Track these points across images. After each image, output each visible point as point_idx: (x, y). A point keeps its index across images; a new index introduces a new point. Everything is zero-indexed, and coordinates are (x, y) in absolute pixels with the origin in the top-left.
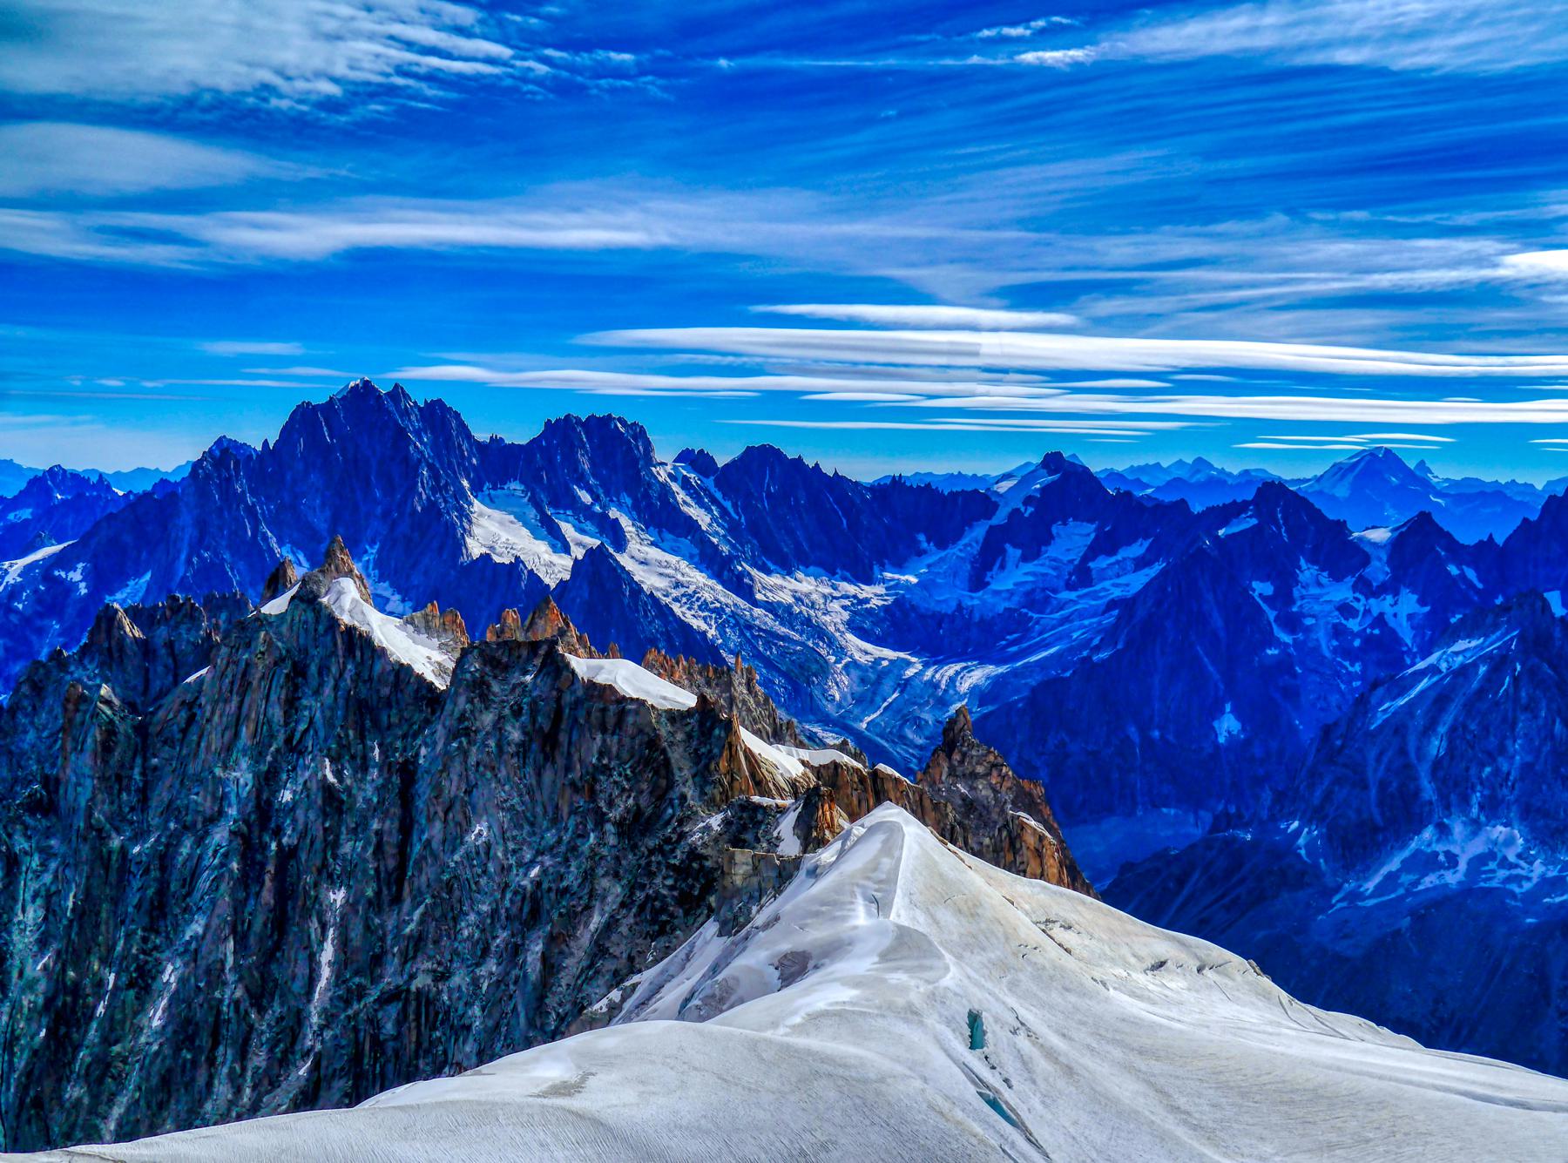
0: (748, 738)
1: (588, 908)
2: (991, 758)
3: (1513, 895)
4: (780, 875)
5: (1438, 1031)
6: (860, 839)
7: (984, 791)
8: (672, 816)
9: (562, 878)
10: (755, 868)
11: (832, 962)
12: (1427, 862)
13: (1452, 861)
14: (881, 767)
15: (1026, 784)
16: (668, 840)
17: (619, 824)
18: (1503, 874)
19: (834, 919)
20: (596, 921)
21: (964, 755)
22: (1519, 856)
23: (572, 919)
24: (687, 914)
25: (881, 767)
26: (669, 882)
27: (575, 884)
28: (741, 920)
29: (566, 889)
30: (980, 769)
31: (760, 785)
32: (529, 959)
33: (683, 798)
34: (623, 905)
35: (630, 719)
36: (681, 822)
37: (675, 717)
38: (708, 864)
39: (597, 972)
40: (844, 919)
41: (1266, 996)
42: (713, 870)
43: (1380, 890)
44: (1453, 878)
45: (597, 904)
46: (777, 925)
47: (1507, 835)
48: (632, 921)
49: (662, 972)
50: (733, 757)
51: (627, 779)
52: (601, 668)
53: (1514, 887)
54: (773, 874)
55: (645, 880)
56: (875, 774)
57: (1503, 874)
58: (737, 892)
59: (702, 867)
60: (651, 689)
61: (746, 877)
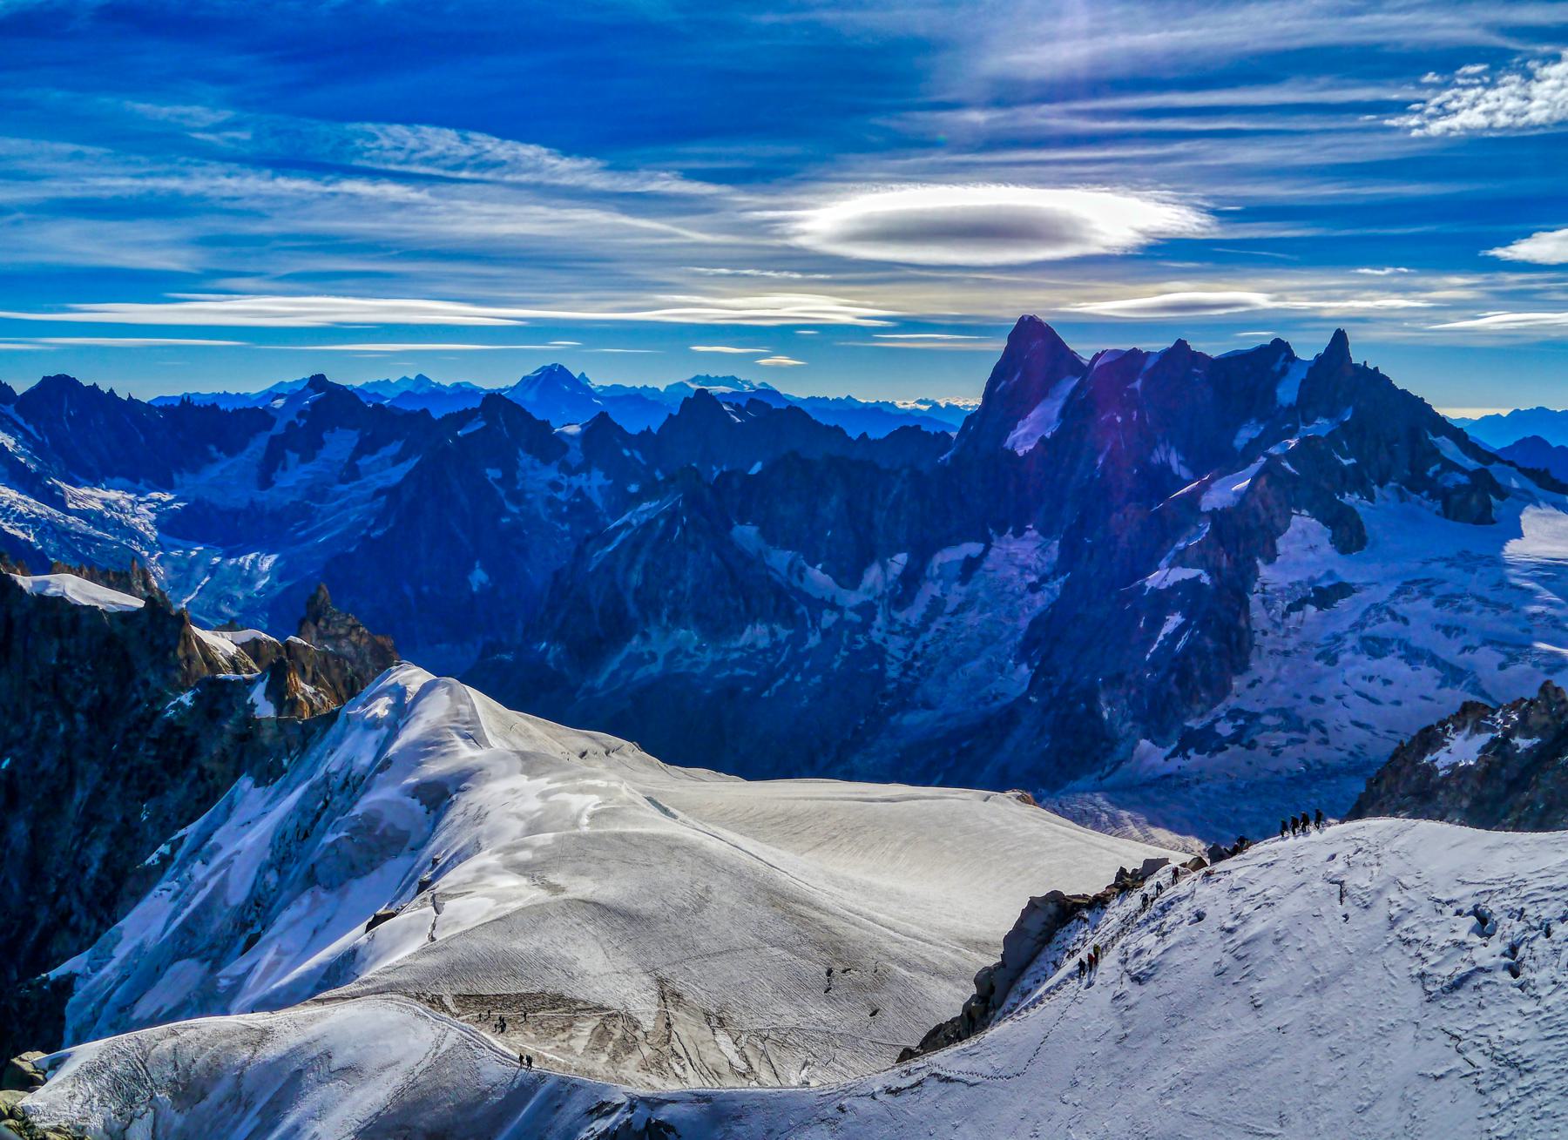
0: (197, 631)
1: (70, 787)
2: (350, 622)
3: (694, 675)
4: (303, 732)
5: (751, 770)
6: (419, 697)
7: (346, 648)
8: (139, 702)
9: (36, 765)
10: (281, 730)
11: (478, 783)
12: (637, 660)
13: (653, 657)
14: (292, 638)
15: (380, 639)
16: (142, 720)
17: (88, 713)
18: (687, 661)
19: (444, 755)
20: (80, 795)
21: (328, 622)
22: (696, 648)
23: (57, 798)
24: (174, 776)
25: (292, 638)
26: (153, 753)
27: (54, 767)
28: (275, 771)
29: (44, 773)
30: (342, 631)
31: (212, 663)
32: (14, 840)
33: (146, 683)
34: (106, 778)
35: (85, 623)
36: (152, 703)
37: (127, 617)
38: (187, 734)
39: (95, 836)
40: (454, 753)
41: (651, 764)
42: (193, 738)
43: (607, 683)
44: (655, 669)
45: (78, 781)
46: (393, 767)
47: (688, 635)
48: (118, 787)
49: (206, 823)
50: (188, 645)
51: (90, 673)
52: (47, 583)
53: (695, 670)
54: (297, 732)
55: (124, 754)
56: (288, 645)
57: (687, 661)
58: (266, 751)
59: (182, 738)
60: (98, 596)
61: (274, 737)
